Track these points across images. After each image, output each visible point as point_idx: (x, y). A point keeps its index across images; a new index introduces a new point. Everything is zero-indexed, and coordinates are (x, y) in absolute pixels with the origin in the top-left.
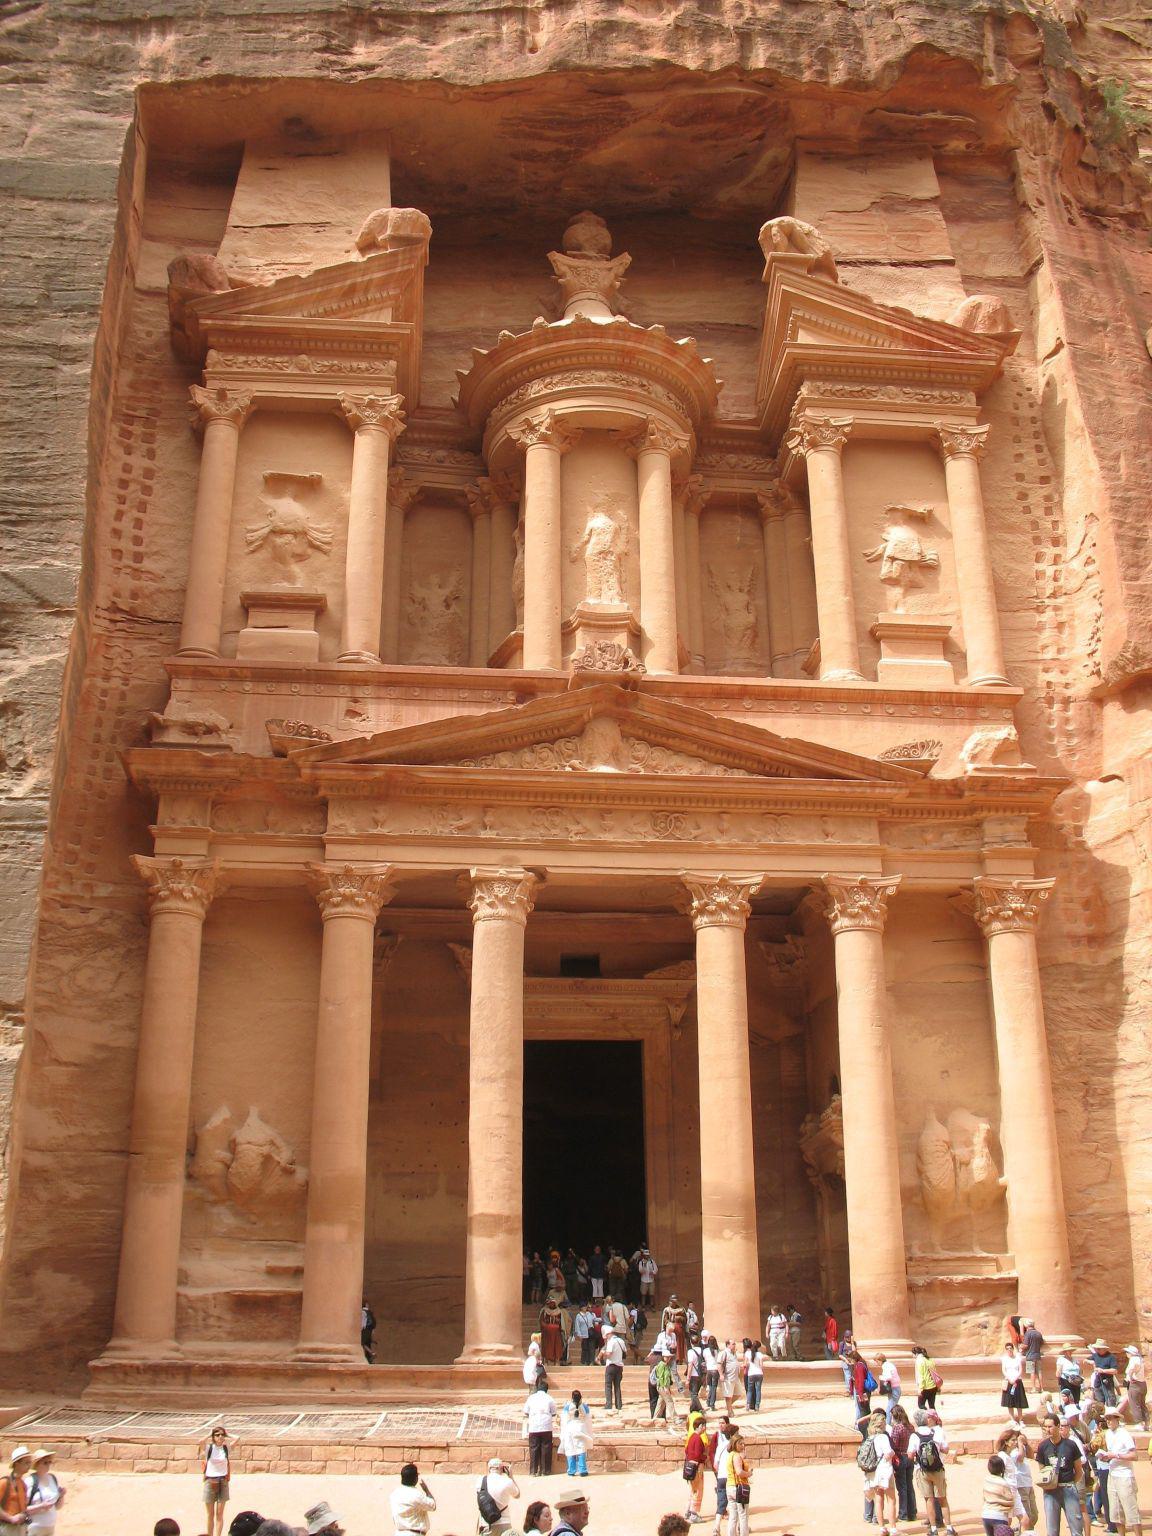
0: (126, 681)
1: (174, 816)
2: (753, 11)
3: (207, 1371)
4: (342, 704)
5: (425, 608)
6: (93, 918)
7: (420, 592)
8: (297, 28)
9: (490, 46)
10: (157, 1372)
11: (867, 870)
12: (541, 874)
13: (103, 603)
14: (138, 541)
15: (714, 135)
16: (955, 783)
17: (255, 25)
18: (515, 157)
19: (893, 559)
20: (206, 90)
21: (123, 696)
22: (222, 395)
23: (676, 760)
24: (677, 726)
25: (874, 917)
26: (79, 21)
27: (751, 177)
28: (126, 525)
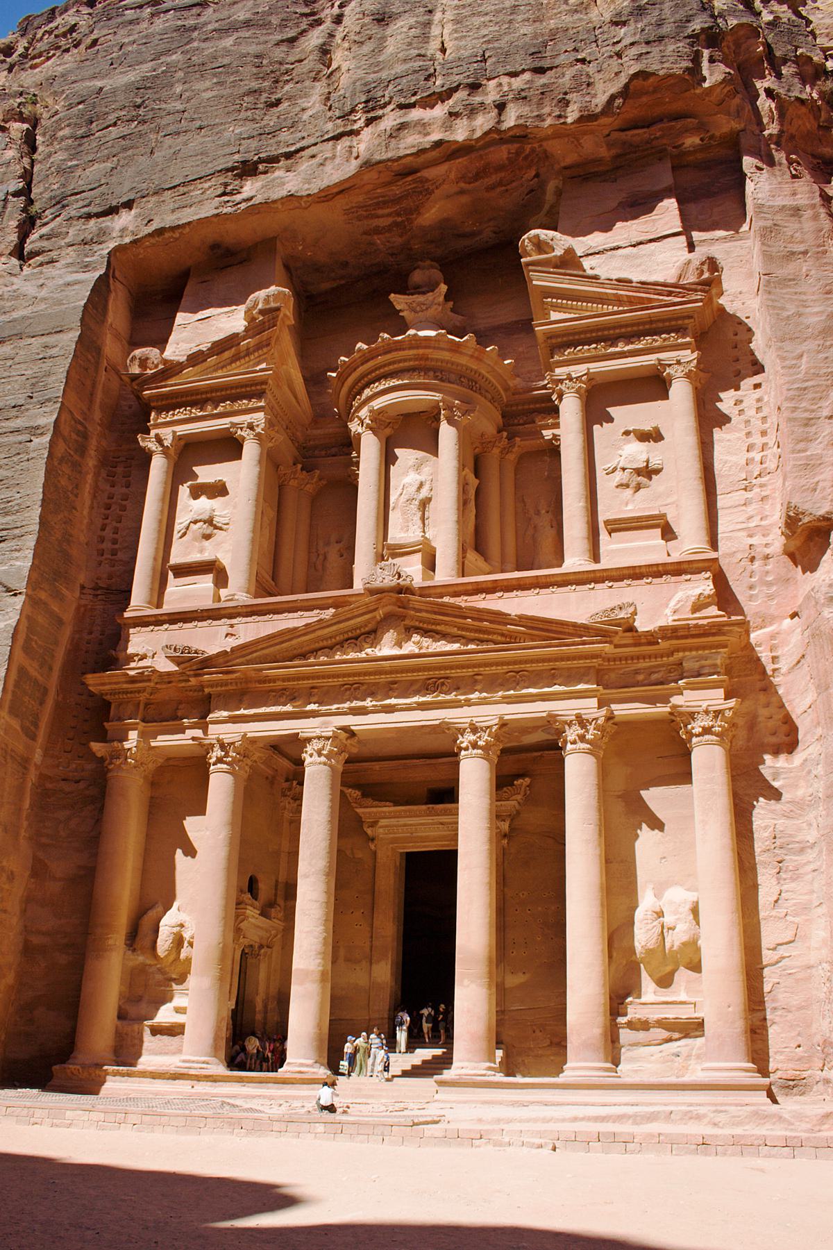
2: (509, 84)
4: (226, 629)
5: (325, 558)
8: (206, 185)
9: (327, 163)
14: (115, 542)
15: (500, 184)
16: (649, 634)
17: (182, 190)
18: (365, 233)
19: (624, 469)
20: (152, 241)
22: (159, 440)
26: (80, 217)
27: (547, 207)
28: (108, 533)
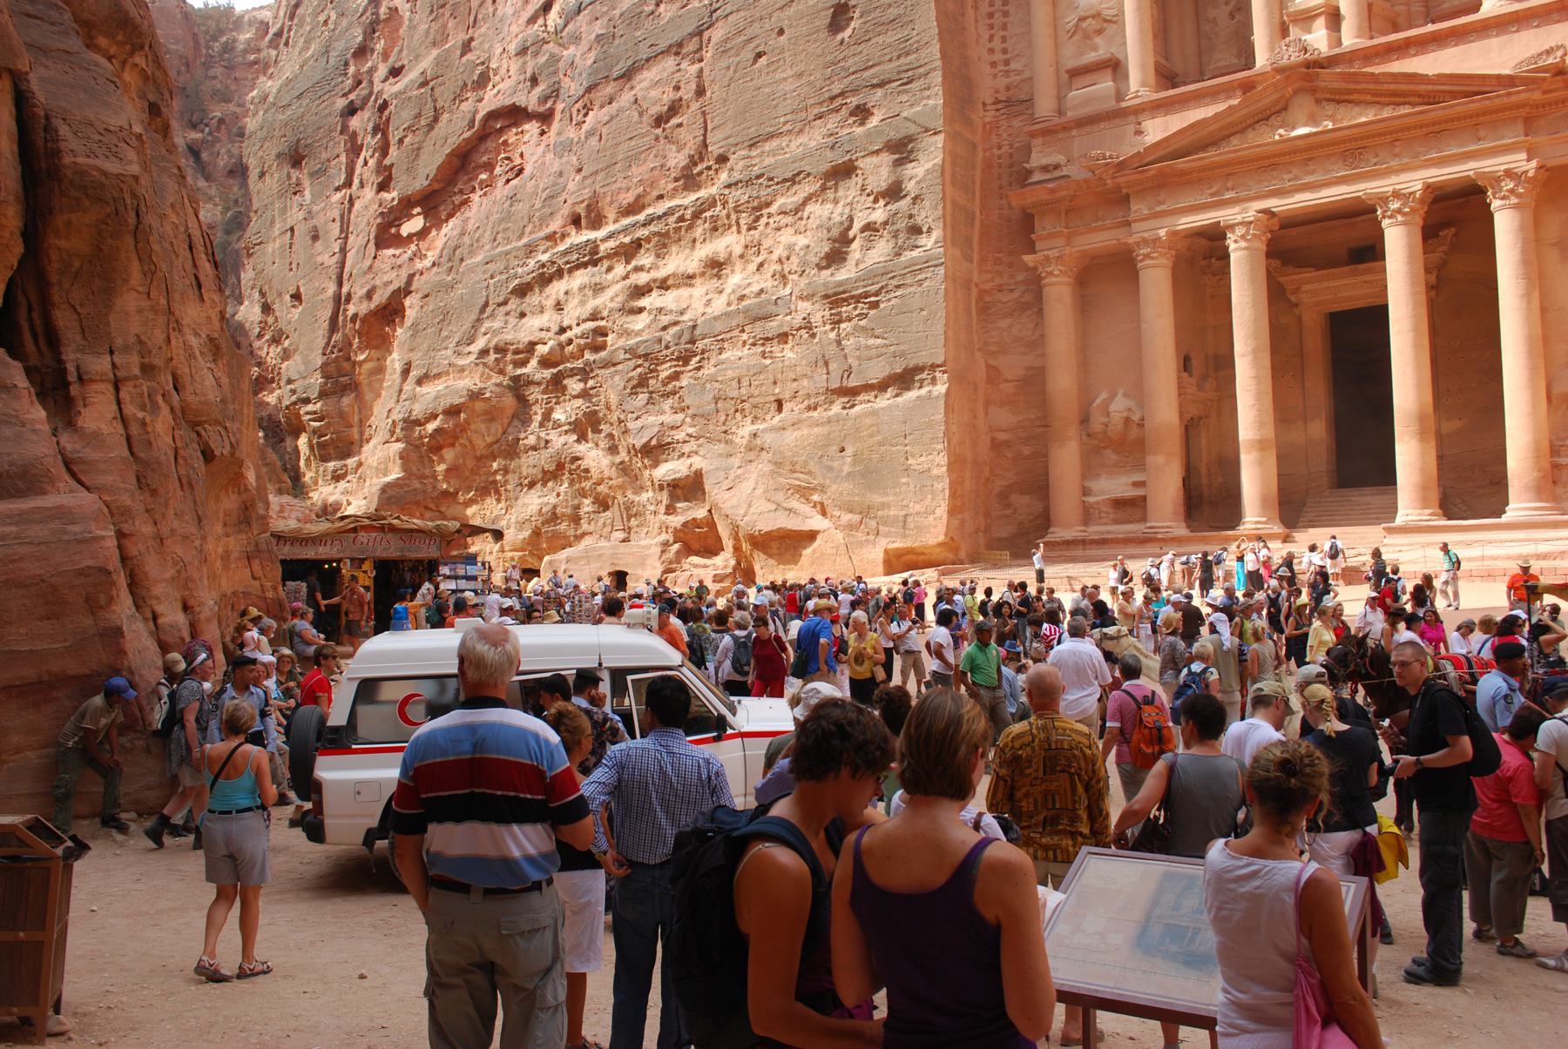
0: (1011, 146)
1: (1044, 227)
3: (1093, 542)
4: (1131, 128)
6: (1016, 294)
7: (1211, 13)
10: (1068, 544)
11: (1520, 161)
12: (1266, 212)
13: (989, 101)
14: (1005, 51)
21: (1011, 155)
23: (1356, 110)
24: (1351, 86)
25: (1519, 196)
28: (997, 44)
